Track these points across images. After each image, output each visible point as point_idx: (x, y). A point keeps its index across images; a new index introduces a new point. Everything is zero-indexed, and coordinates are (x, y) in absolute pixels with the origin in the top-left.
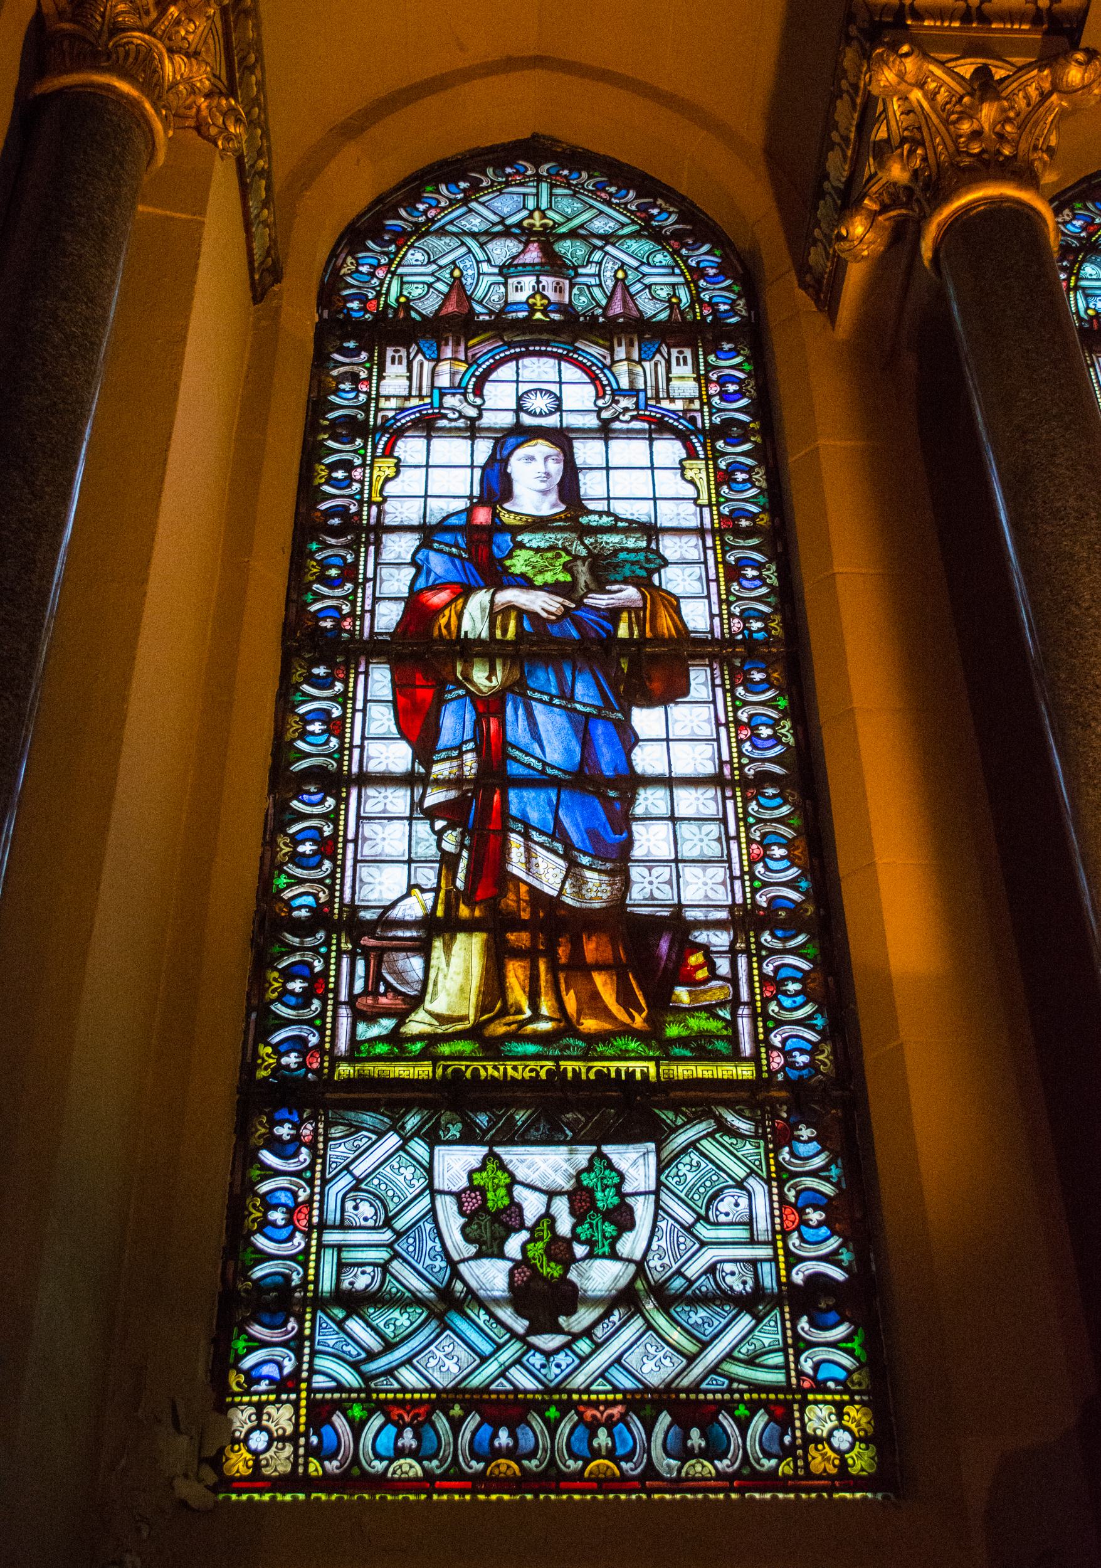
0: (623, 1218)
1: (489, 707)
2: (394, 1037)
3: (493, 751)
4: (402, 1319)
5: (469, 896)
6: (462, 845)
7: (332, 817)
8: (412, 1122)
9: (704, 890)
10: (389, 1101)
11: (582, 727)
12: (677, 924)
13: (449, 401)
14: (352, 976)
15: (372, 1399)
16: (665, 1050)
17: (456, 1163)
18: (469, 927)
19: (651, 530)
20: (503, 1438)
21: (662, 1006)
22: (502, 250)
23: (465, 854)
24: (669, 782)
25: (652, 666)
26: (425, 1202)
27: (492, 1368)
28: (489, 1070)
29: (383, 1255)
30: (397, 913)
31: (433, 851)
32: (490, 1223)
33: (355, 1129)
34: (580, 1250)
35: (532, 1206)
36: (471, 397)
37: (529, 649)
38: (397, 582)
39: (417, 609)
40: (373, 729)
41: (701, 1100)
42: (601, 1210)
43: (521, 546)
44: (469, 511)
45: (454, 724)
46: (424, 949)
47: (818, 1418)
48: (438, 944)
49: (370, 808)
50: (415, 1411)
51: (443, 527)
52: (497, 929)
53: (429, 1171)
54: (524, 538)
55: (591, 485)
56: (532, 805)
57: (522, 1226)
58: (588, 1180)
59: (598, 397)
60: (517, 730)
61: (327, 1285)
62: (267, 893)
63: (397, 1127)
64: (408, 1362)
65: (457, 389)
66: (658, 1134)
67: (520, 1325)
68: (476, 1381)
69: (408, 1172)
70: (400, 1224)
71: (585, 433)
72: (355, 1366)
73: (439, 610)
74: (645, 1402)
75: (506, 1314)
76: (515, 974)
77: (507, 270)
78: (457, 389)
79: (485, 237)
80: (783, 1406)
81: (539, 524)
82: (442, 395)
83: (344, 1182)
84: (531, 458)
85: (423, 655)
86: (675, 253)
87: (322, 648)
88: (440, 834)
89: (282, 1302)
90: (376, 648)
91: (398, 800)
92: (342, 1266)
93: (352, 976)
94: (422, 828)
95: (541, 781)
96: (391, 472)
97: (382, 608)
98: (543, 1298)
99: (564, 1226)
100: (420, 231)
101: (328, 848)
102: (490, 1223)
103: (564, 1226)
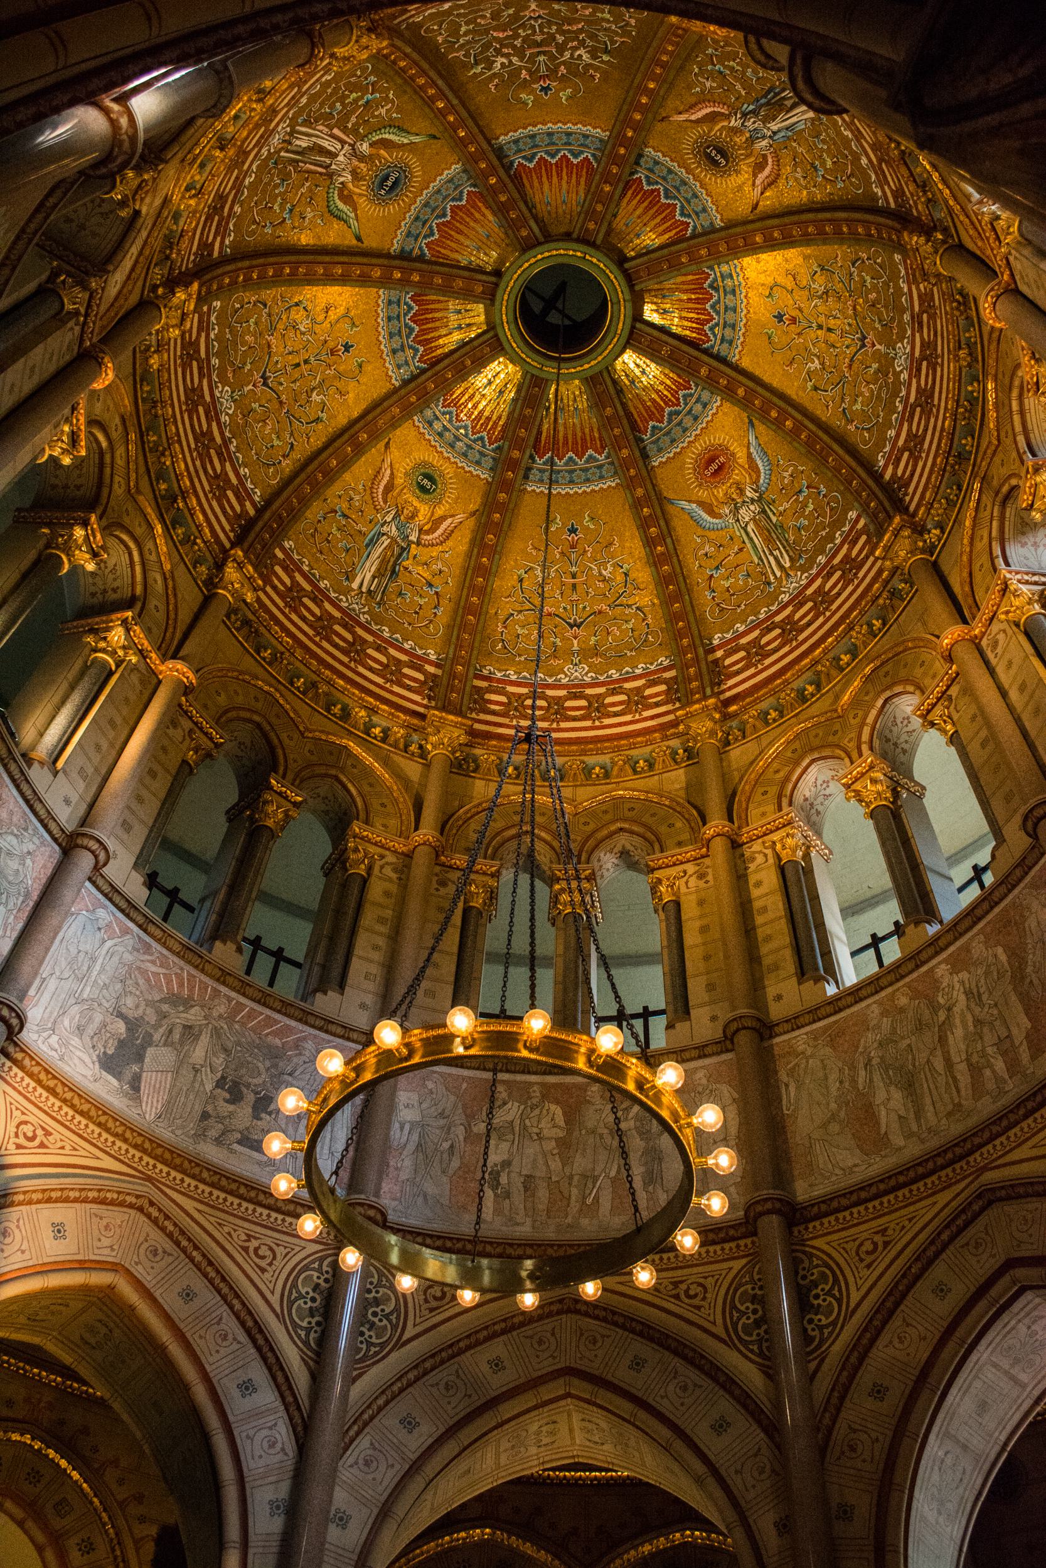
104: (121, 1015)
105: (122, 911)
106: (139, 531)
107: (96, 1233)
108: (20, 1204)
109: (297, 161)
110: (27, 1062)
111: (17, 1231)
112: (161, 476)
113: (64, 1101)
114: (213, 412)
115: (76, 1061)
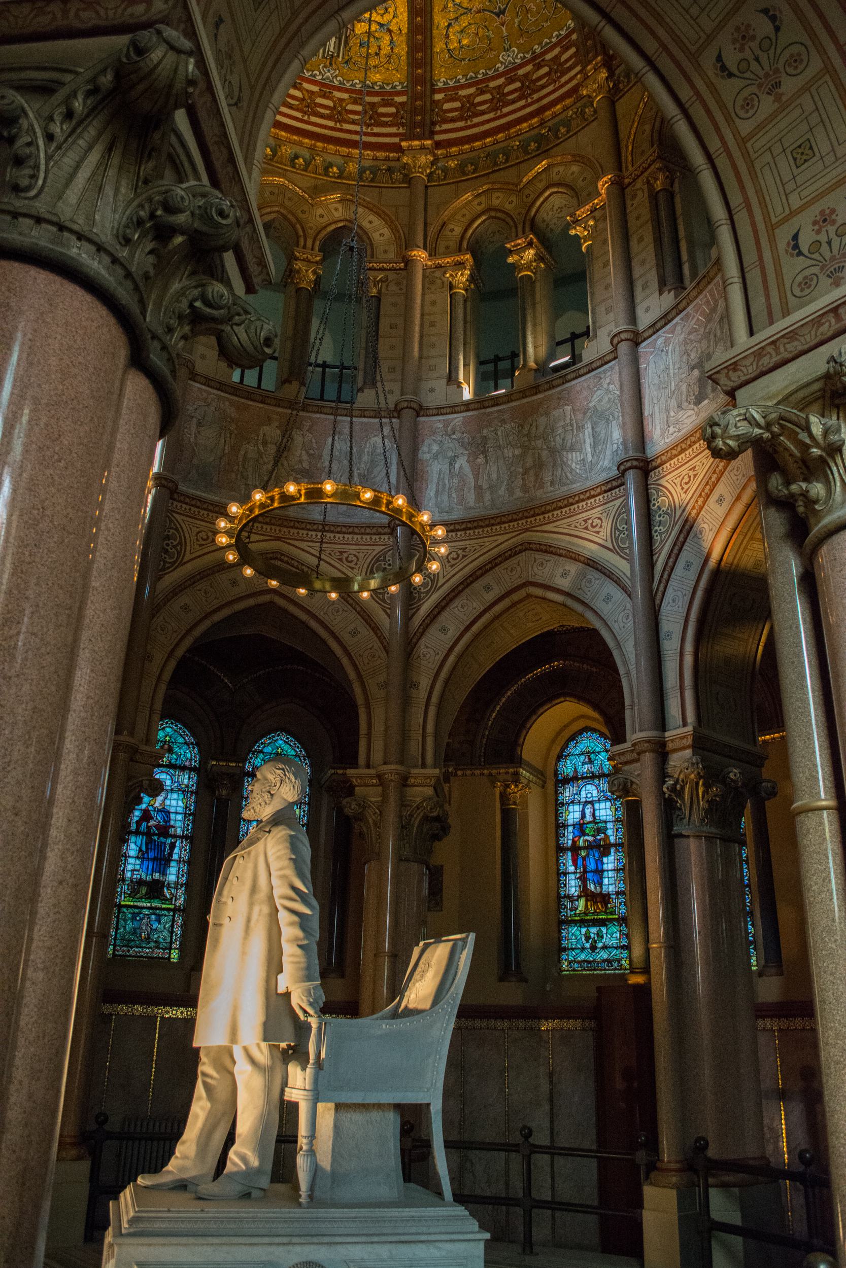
0: (602, 937)
1: (584, 859)
3: (585, 867)
5: (583, 892)
9: (612, 889)
10: (575, 922)
11: (596, 861)
12: (609, 895)
14: (569, 905)
15: (575, 961)
16: (606, 914)
17: (584, 930)
19: (605, 822)
21: (607, 908)
22: (582, 758)
24: (607, 871)
25: (605, 849)
35: (592, 935)
37: (589, 847)
38: (571, 836)
39: (574, 842)
41: (611, 920)
42: (600, 936)
45: (580, 862)
47: (623, 962)
52: (586, 896)
55: (597, 813)
56: (589, 876)
60: (588, 864)
62: (559, 894)
65: (577, 794)
66: (605, 925)
74: (604, 961)
76: (589, 904)
77: (583, 764)
78: (577, 794)
80: (619, 961)
81: (589, 822)
85: (575, 849)
87: (561, 849)
89: (565, 949)
90: (568, 849)
91: (573, 876)
93: (569, 905)
98: (593, 948)
100: (569, 755)
101: (565, 885)
102: (588, 938)
104: (693, 368)
105: (666, 324)
106: (541, 186)
107: (735, 478)
108: (698, 514)
109: (347, 37)
110: (664, 458)
111: (705, 526)
112: (524, 147)
113: (690, 446)
114: (510, 74)
115: (686, 421)
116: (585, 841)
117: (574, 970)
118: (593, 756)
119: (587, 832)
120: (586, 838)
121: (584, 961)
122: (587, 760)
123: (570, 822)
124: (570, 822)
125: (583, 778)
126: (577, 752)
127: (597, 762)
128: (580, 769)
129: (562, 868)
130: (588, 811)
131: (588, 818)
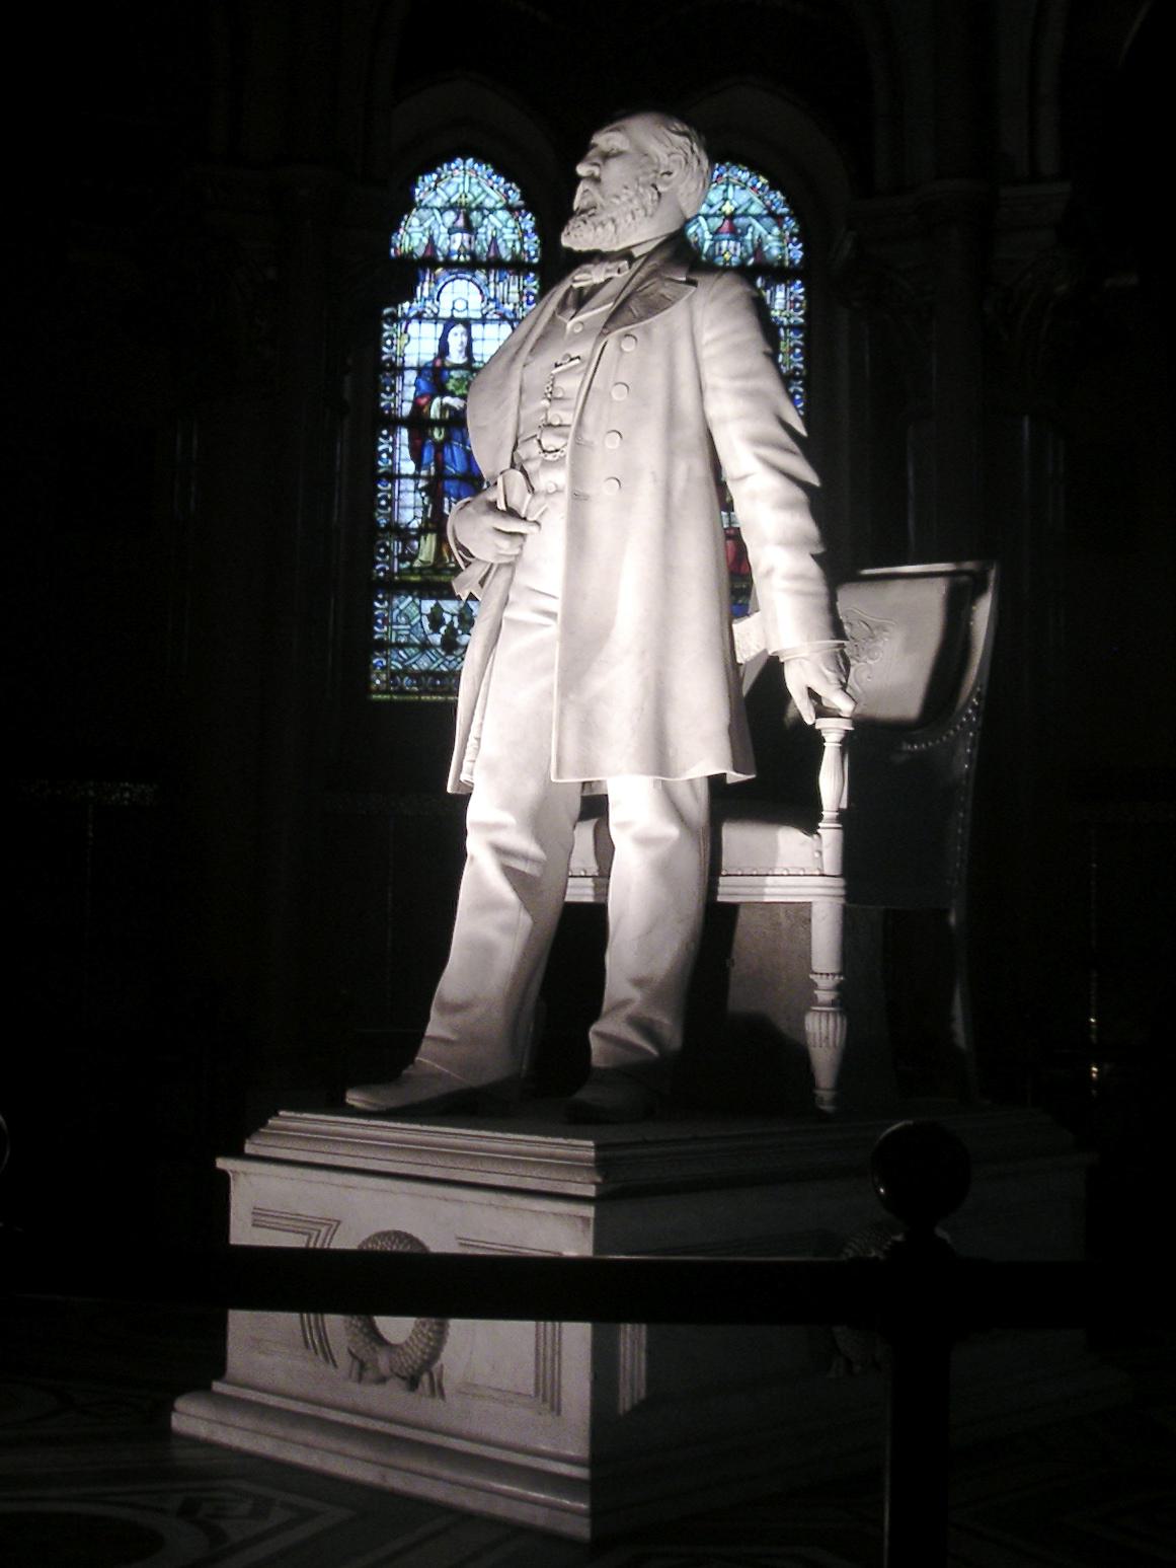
1: (439, 447)
2: (411, 568)
3: (440, 466)
4: (413, 651)
6: (429, 502)
7: (391, 491)
8: (415, 593)
10: (406, 588)
13: (429, 304)
15: (406, 671)
17: (428, 605)
18: (432, 531)
20: (438, 682)
22: (450, 217)
23: (431, 506)
26: (418, 618)
27: (435, 665)
28: (436, 578)
29: (407, 632)
30: (411, 526)
31: (421, 504)
32: (436, 620)
33: (399, 595)
34: (460, 632)
35: (447, 618)
36: (436, 301)
38: (410, 393)
40: (403, 457)
43: (451, 377)
44: (434, 361)
45: (428, 454)
46: (418, 539)
48: (423, 537)
49: (402, 488)
50: (417, 676)
51: (426, 367)
53: (419, 607)
54: (453, 373)
55: (476, 348)
57: (444, 624)
58: (463, 612)
59: (483, 301)
60: (448, 457)
61: (393, 640)
63: (411, 594)
64: (415, 663)
67: (443, 653)
68: (432, 668)
69: (414, 608)
70: (413, 623)
71: (477, 321)
72: (402, 663)
73: (423, 407)
75: (440, 650)
77: (451, 232)
79: (442, 210)
81: (457, 367)
82: (425, 300)
83: (397, 611)
84: (456, 334)
85: (418, 423)
86: (517, 220)
88: (423, 498)
89: (383, 646)
91: (409, 485)
92: (398, 636)
93: (397, 547)
94: (418, 495)
95: (453, 478)
96: (406, 341)
97: (404, 405)
99: (456, 625)
101: (390, 503)
103: (456, 625)
116: (444, 408)
117: (402, 691)
118: (475, 216)
119: (450, 386)
120: (447, 400)
121: (428, 673)
122: (461, 223)
123: (411, 361)
124: (411, 361)
125: (448, 264)
126: (438, 203)
127: (485, 233)
128: (442, 242)
129: (383, 464)
130: (456, 339)
131: (456, 357)
